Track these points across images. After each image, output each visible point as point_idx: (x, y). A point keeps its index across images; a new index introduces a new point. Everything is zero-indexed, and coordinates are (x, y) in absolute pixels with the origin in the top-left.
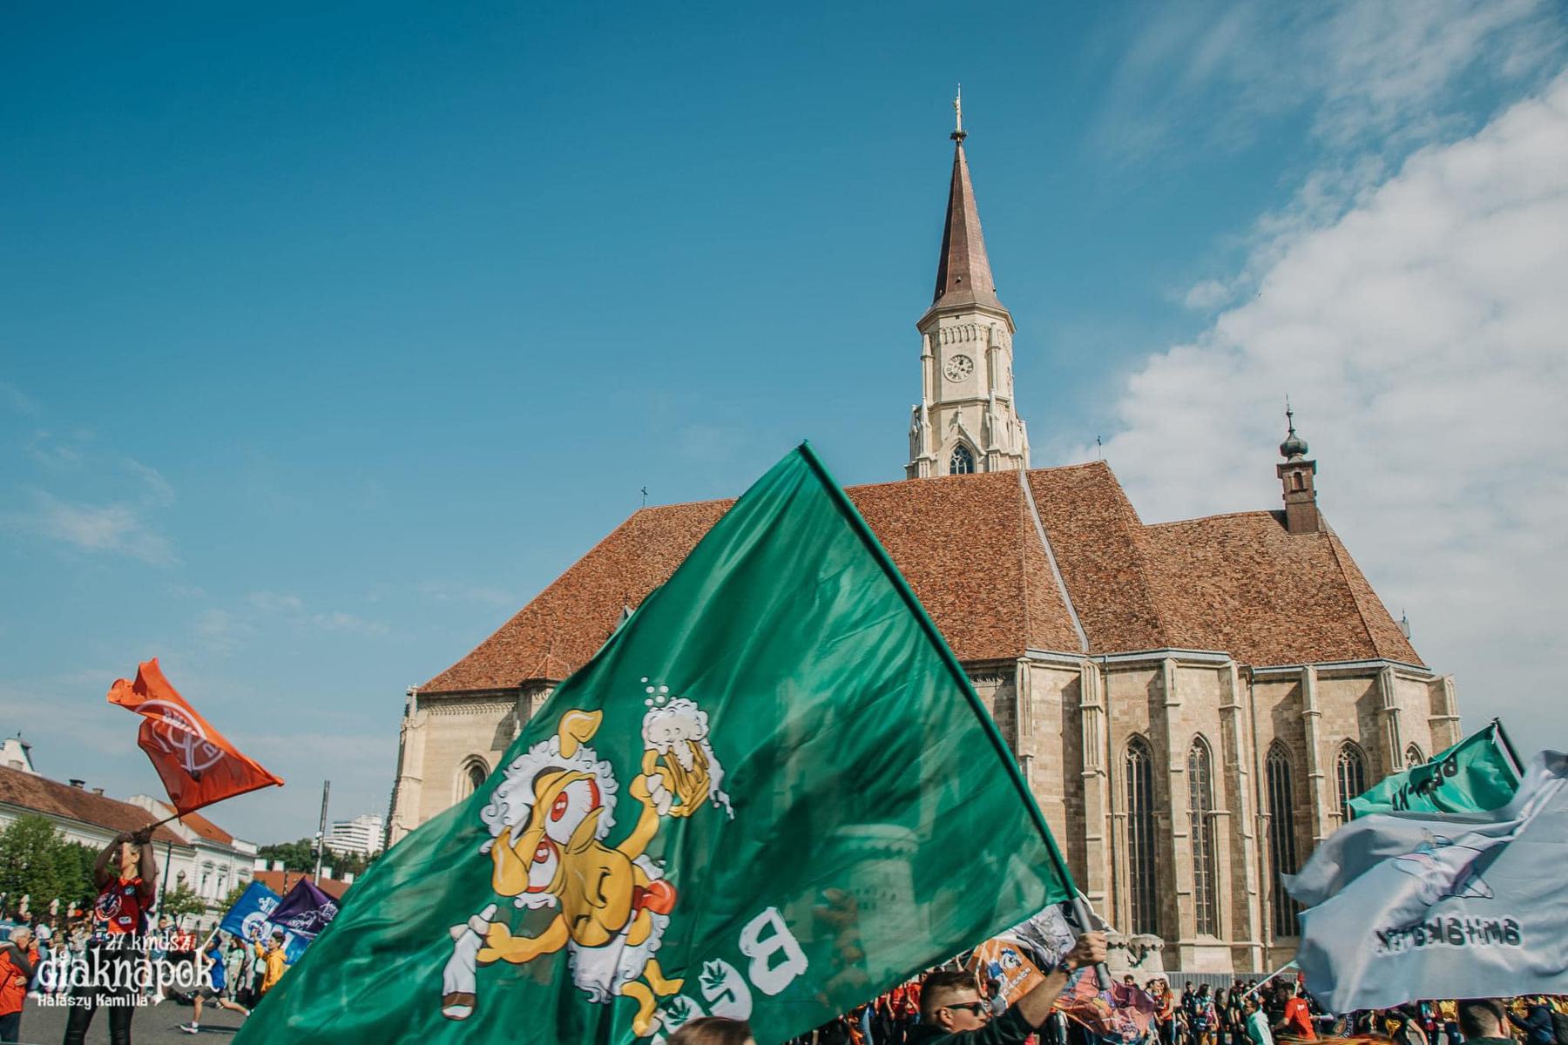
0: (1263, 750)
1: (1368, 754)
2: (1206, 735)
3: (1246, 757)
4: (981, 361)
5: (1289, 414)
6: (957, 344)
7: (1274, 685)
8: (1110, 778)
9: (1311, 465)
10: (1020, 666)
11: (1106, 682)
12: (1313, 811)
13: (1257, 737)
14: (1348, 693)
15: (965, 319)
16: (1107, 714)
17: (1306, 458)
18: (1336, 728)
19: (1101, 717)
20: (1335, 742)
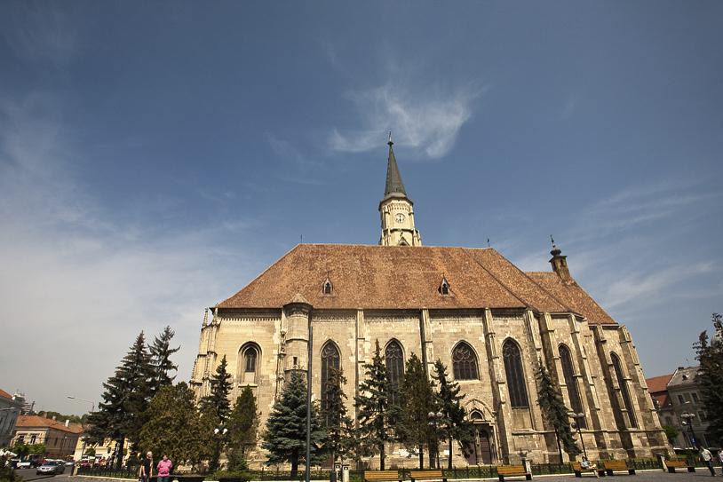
9: (564, 257)
17: (561, 255)
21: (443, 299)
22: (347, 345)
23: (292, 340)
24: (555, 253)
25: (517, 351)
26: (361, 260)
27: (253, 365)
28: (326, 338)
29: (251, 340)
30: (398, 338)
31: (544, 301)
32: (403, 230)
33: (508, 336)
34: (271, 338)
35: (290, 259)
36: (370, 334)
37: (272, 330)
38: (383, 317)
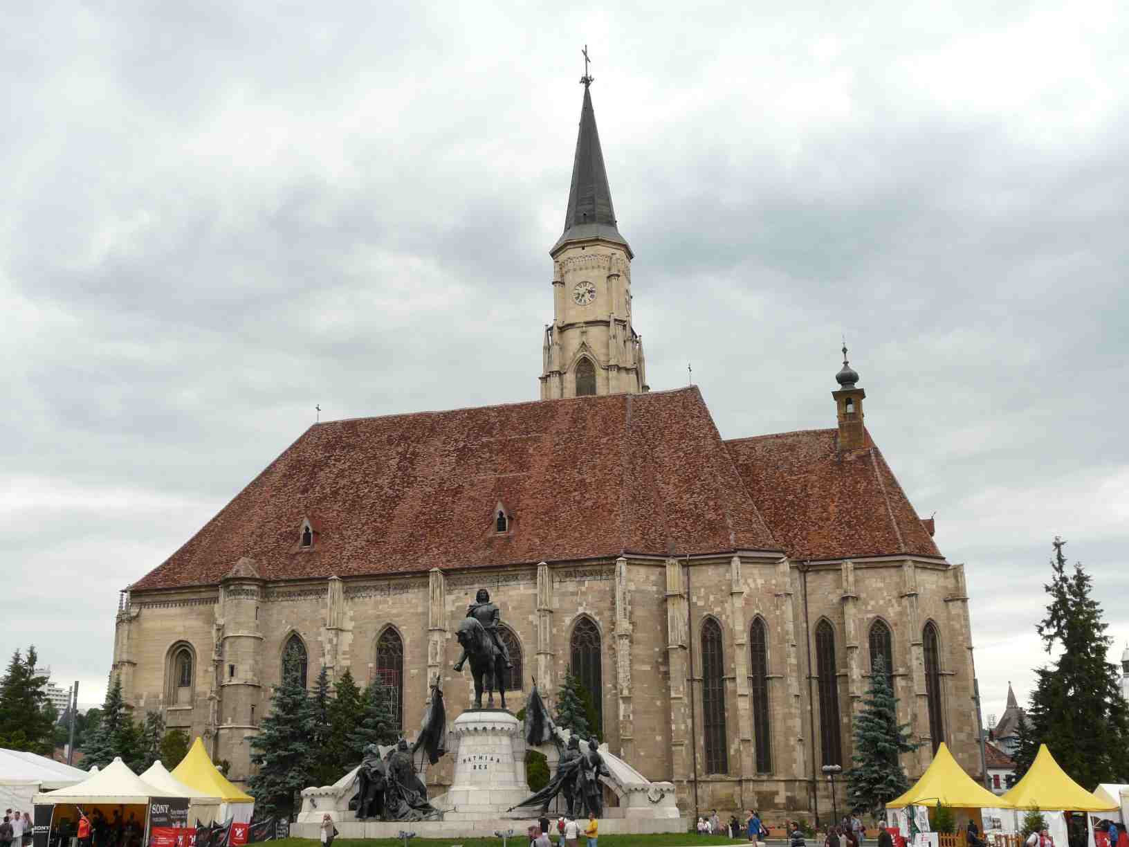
0: (811, 625)
1: (893, 628)
2: (764, 615)
3: (797, 634)
4: (601, 285)
5: (845, 350)
6: (584, 272)
7: (822, 573)
8: (691, 650)
9: (861, 394)
10: (618, 564)
11: (688, 574)
12: (849, 674)
13: (809, 616)
14: (879, 580)
15: (589, 250)
16: (688, 600)
17: (857, 386)
18: (869, 608)
19: (684, 604)
20: (867, 619)
21: (489, 543)
22: (316, 638)
23: (228, 637)
24: (847, 379)
25: (598, 639)
26: (403, 456)
27: (189, 675)
28: (288, 629)
29: (182, 638)
30: (396, 622)
31: (710, 522)
32: (589, 323)
33: (581, 610)
34: (210, 632)
35: (282, 468)
36: (352, 619)
37: (210, 620)
38: (376, 588)
